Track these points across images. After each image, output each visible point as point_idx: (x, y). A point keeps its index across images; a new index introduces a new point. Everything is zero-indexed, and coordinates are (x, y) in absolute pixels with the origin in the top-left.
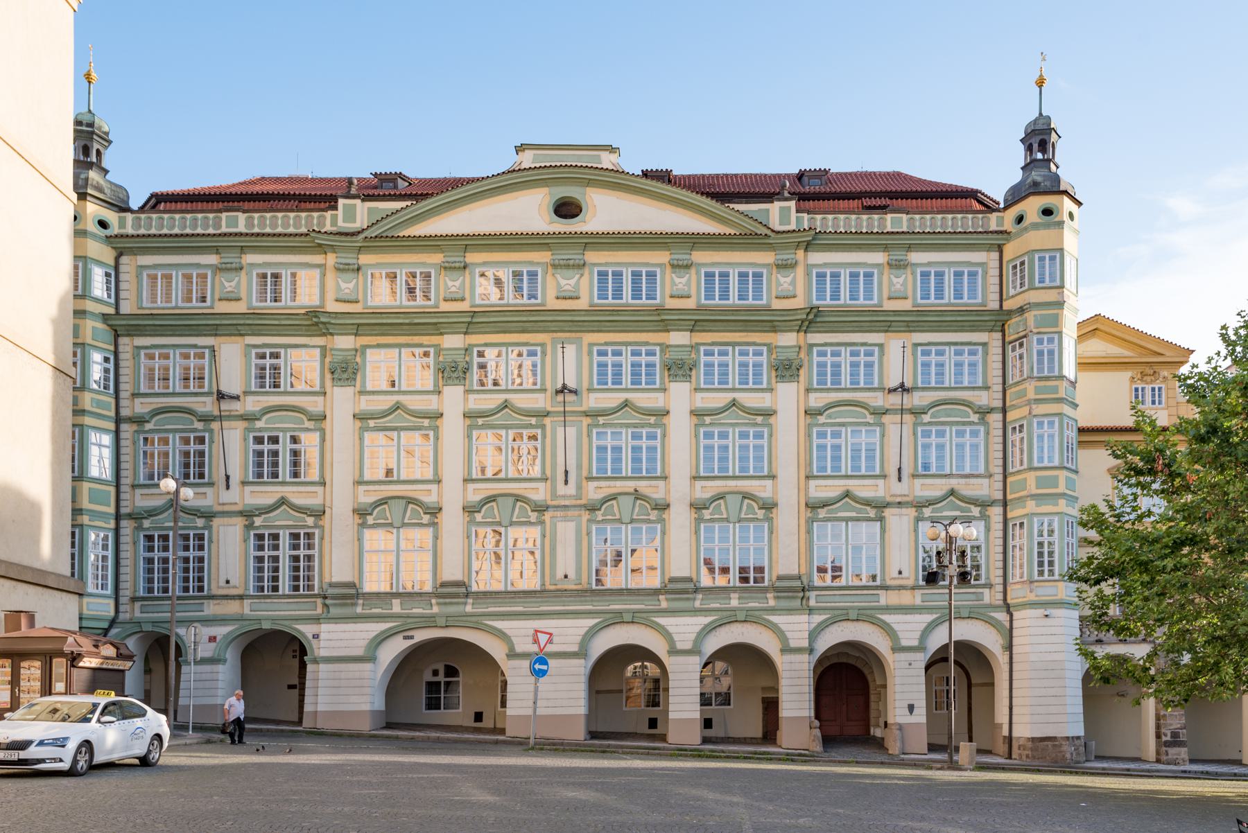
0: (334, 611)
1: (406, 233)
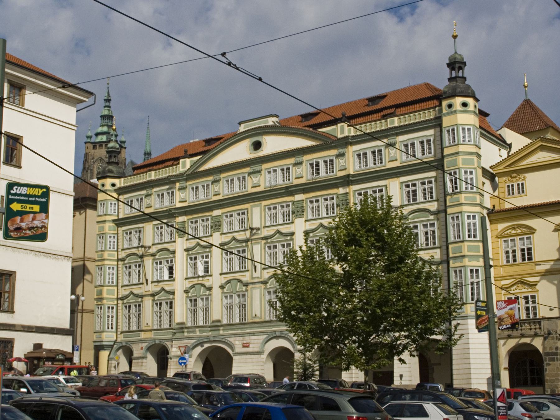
0: (178, 335)
1: (202, 169)
